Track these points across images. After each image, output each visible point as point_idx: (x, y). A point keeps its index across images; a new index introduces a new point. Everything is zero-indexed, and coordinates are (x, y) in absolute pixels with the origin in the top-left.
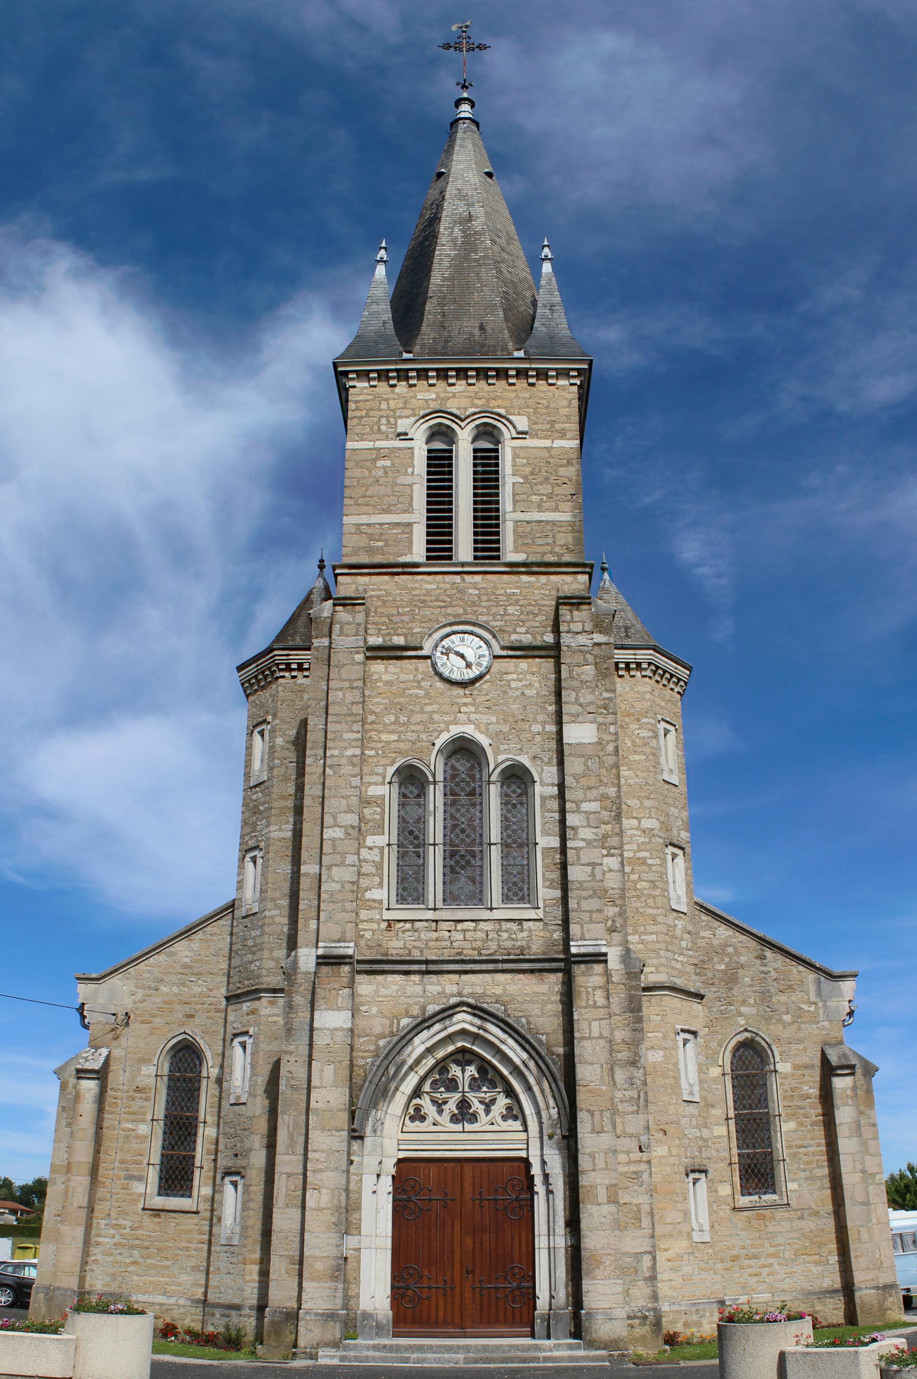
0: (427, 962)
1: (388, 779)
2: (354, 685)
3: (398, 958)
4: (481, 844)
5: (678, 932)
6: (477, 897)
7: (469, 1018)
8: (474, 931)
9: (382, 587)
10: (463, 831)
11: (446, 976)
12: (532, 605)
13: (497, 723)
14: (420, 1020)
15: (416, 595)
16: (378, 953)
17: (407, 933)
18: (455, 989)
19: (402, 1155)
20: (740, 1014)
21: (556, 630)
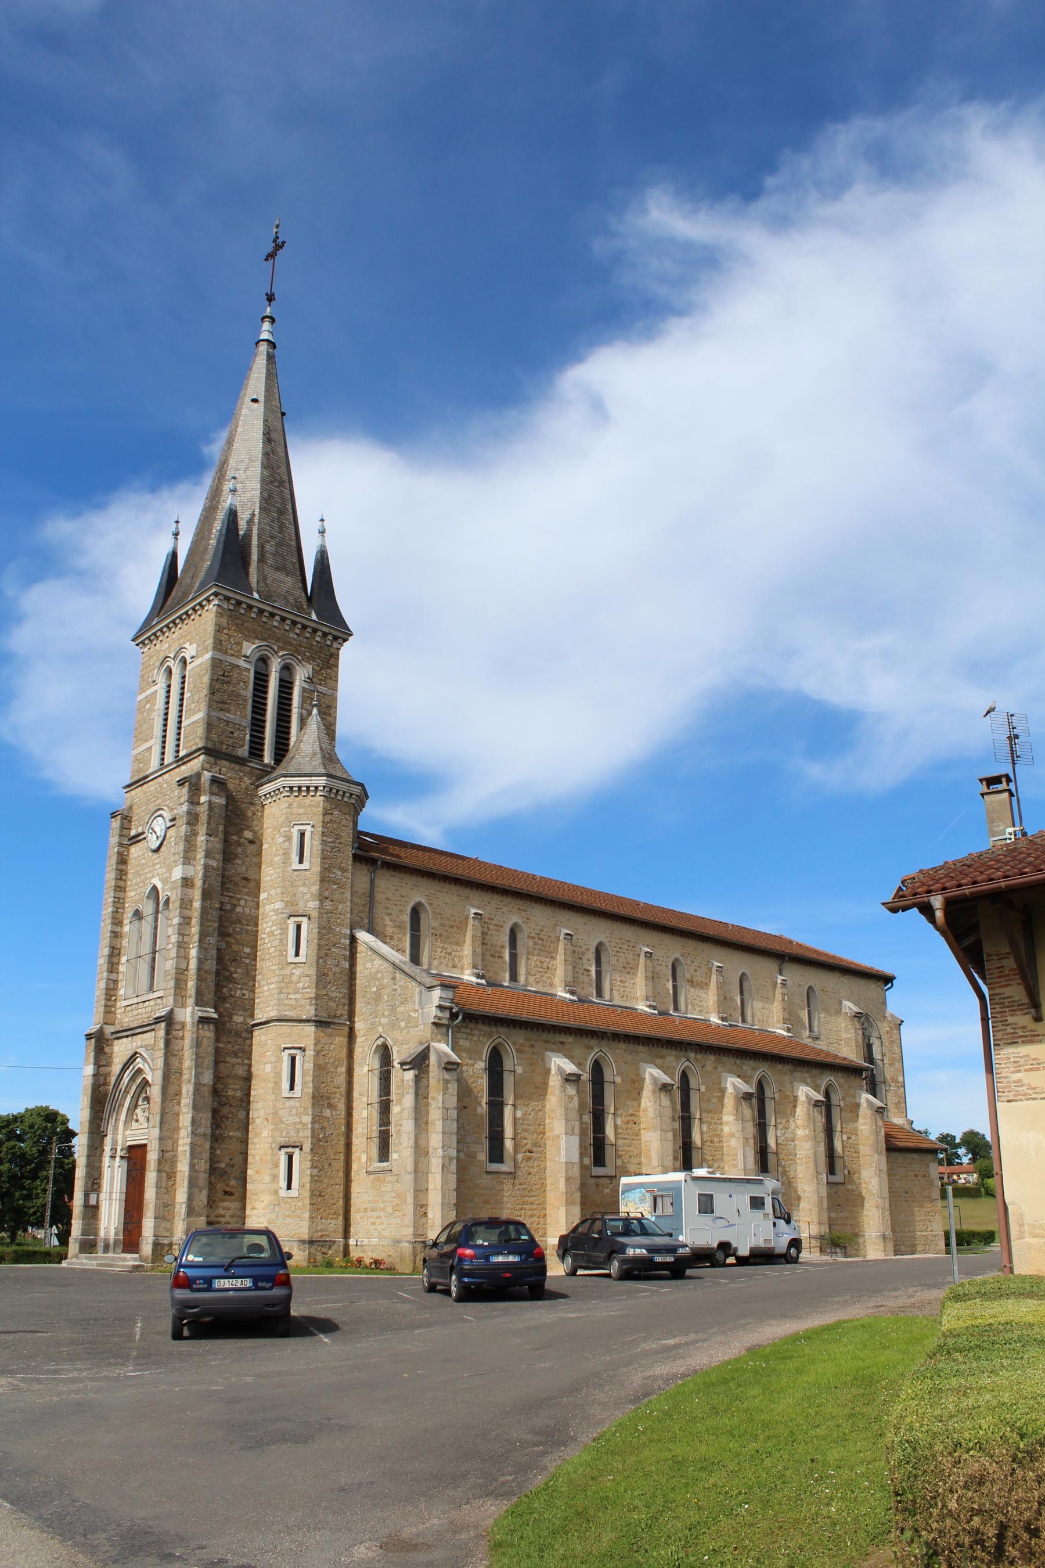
5: (295, 978)
19: (129, 1143)
20: (380, 1024)
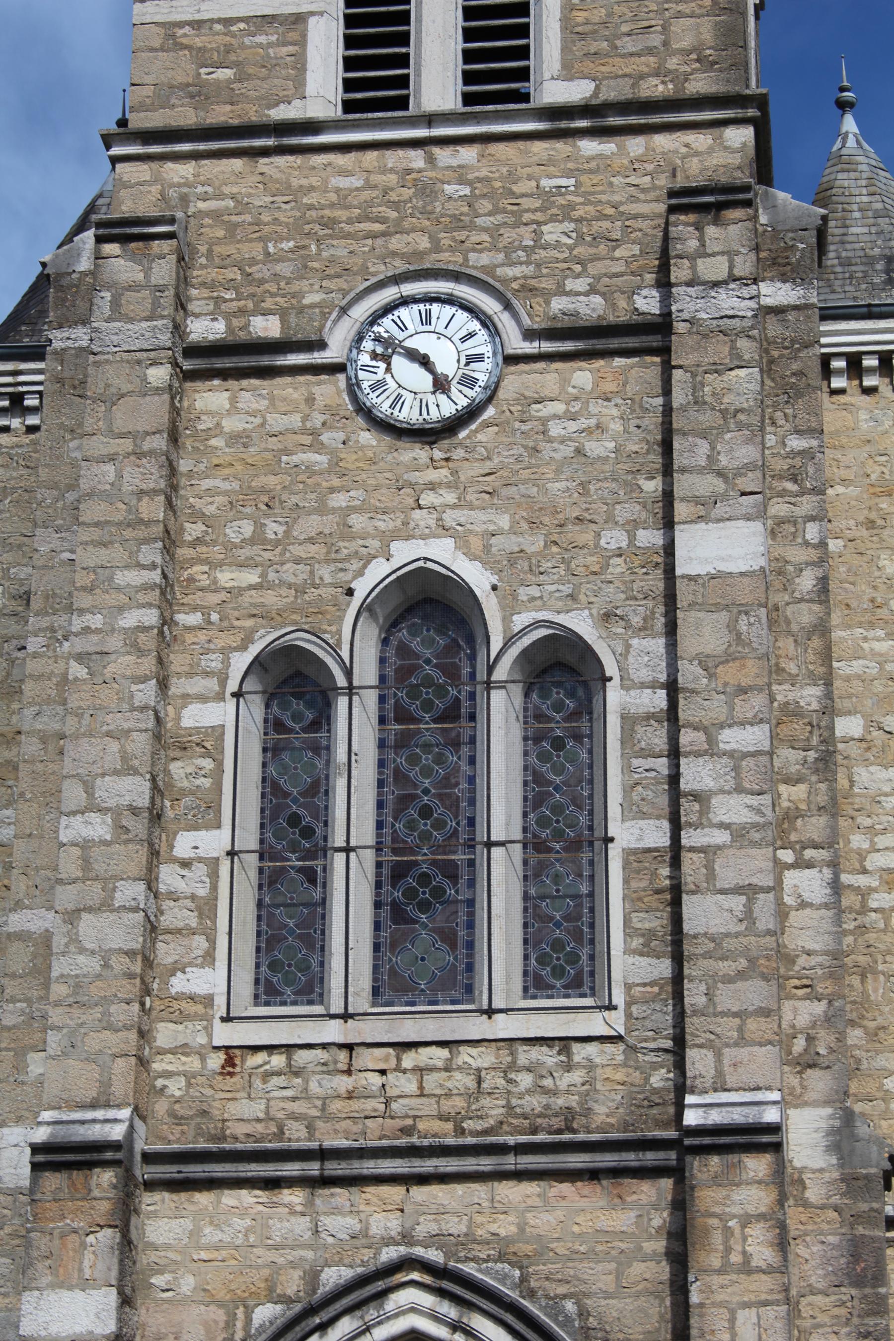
0: (323, 1154)
1: (233, 685)
2: (146, 446)
3: (250, 1146)
4: (471, 845)
6: (458, 983)
7: (427, 1300)
8: (447, 1069)
9: (227, 190)
10: (426, 812)
11: (371, 1189)
12: (607, 217)
13: (513, 531)
14: (298, 1308)
15: (311, 207)
16: (199, 1132)
17: (276, 1081)
18: (393, 1224)
21: (664, 284)
